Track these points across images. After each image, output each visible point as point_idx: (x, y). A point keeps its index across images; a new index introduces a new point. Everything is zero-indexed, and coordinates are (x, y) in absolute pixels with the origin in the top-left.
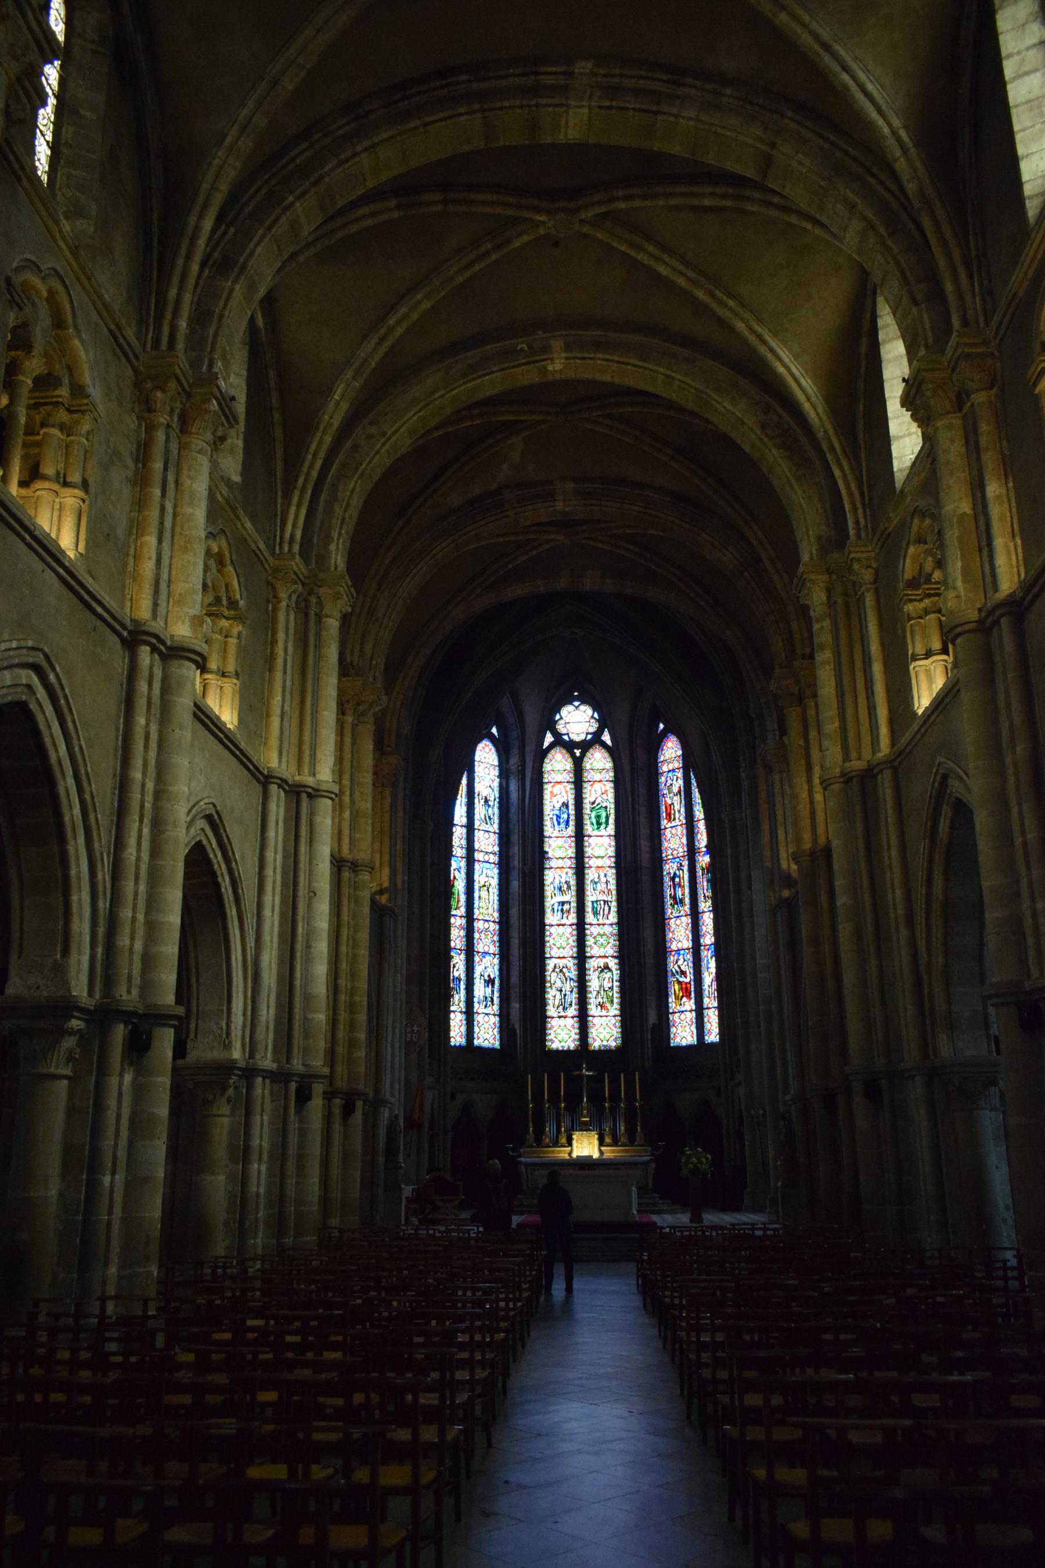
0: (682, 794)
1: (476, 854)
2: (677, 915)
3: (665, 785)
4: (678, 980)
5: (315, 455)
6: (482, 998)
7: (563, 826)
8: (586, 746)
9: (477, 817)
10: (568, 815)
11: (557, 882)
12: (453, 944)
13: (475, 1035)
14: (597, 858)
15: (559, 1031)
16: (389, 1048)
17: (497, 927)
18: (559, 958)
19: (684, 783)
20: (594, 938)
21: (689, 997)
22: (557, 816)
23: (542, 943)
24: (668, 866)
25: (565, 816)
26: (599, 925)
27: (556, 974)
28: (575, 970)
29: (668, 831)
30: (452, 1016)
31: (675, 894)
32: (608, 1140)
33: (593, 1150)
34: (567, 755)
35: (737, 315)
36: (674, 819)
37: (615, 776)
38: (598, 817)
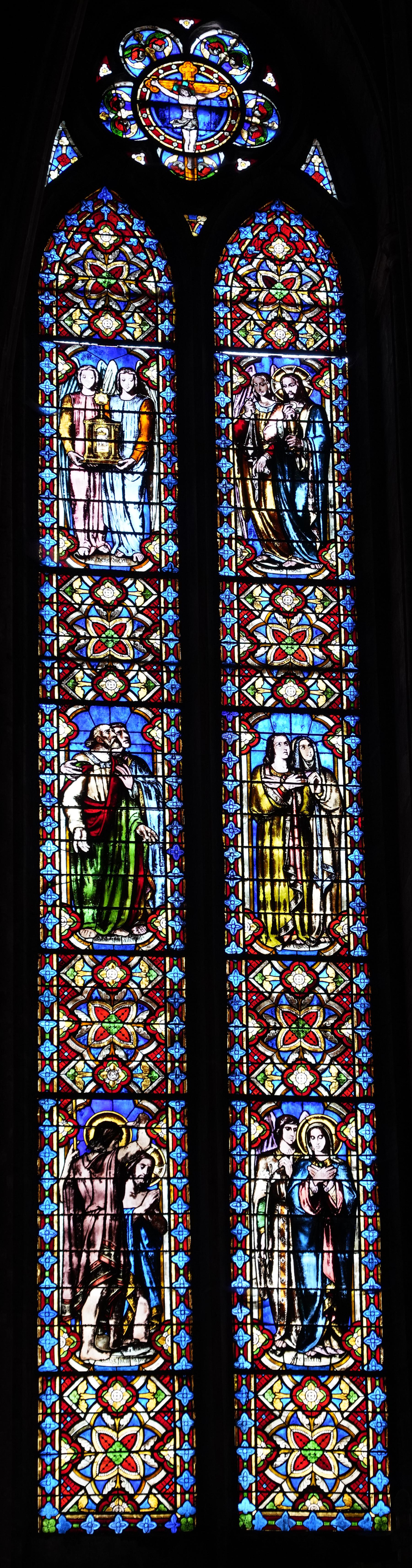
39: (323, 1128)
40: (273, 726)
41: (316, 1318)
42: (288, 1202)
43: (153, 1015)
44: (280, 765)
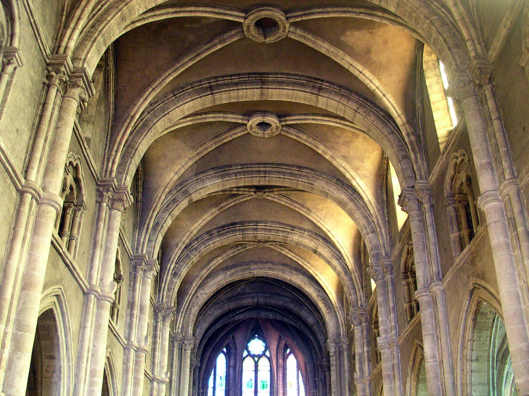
5: (186, 302)
8: (259, 357)
25: (250, 384)
34: (253, 360)
35: (310, 268)
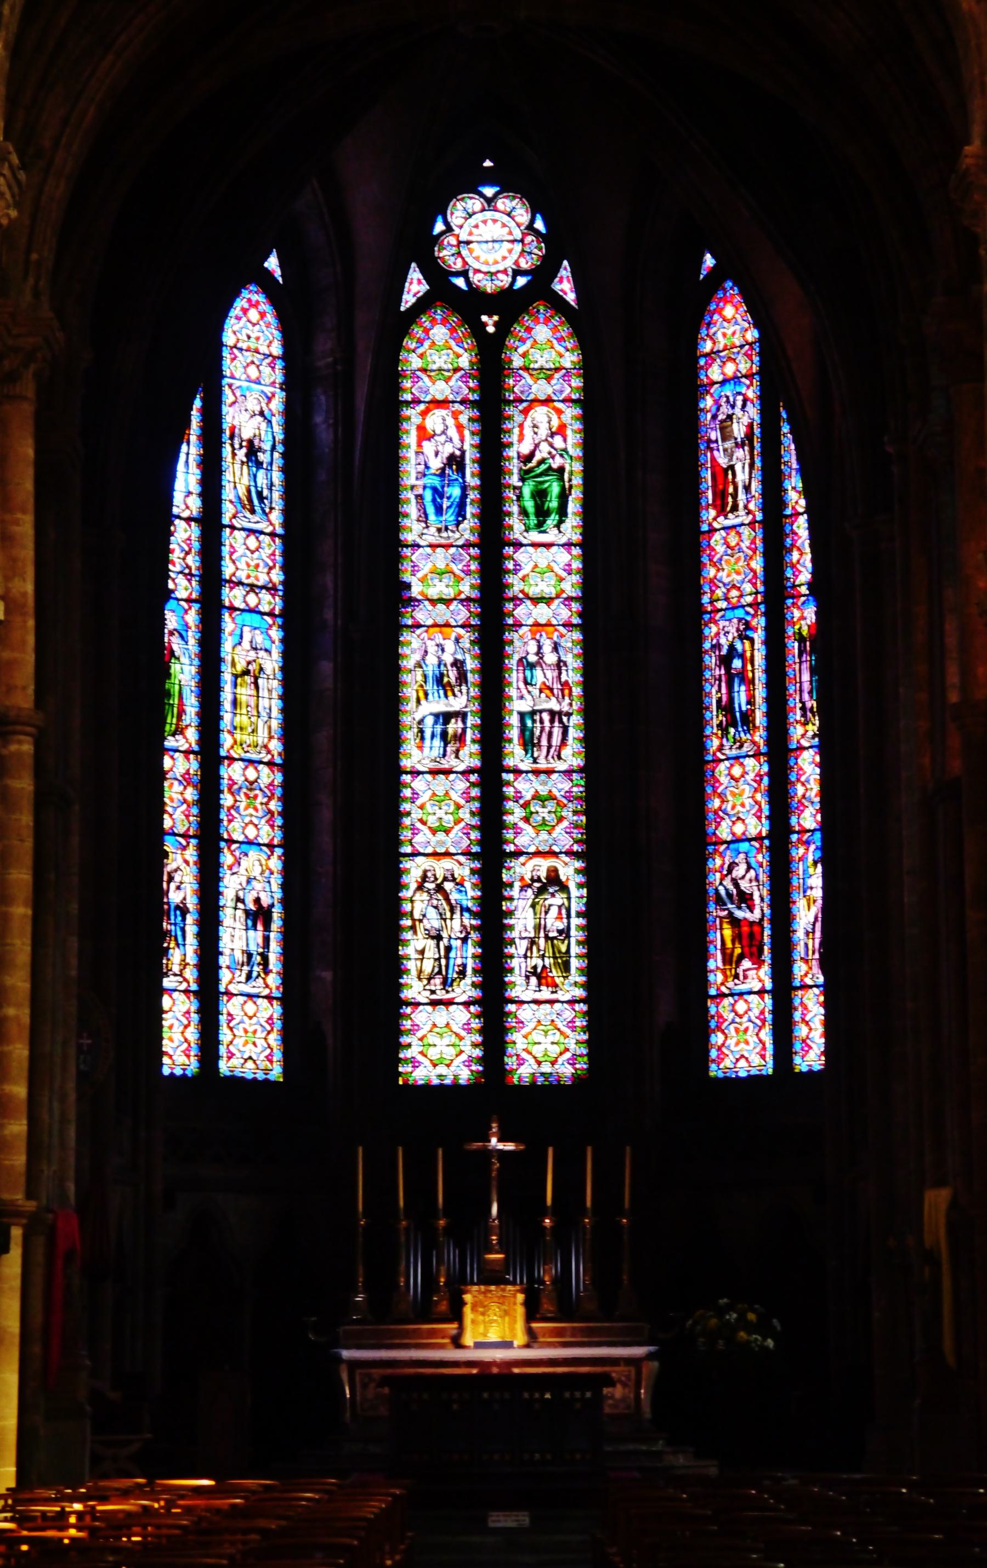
0: (757, 446)
1: (226, 591)
2: (734, 752)
3: (714, 417)
4: (731, 914)
6: (239, 956)
7: (449, 517)
9: (228, 493)
10: (464, 488)
11: (432, 660)
12: (167, 823)
13: (223, 1050)
14: (536, 601)
15: (431, 1039)
16: (56, 1105)
17: (279, 778)
18: (435, 854)
19: (763, 413)
20: (525, 805)
21: (759, 962)
22: (434, 490)
23: (394, 817)
24: (714, 629)
25: (455, 492)
26: (537, 772)
27: (425, 896)
28: (475, 886)
29: (717, 536)
30: (166, 1002)
31: (731, 699)
32: (547, 1306)
33: (512, 1329)
36: (735, 508)
37: (586, 389)
38: (540, 495)
39: (259, 860)
40: (243, 620)
41: (252, 966)
42: (243, 901)
43: (185, 788)
44: (246, 644)
